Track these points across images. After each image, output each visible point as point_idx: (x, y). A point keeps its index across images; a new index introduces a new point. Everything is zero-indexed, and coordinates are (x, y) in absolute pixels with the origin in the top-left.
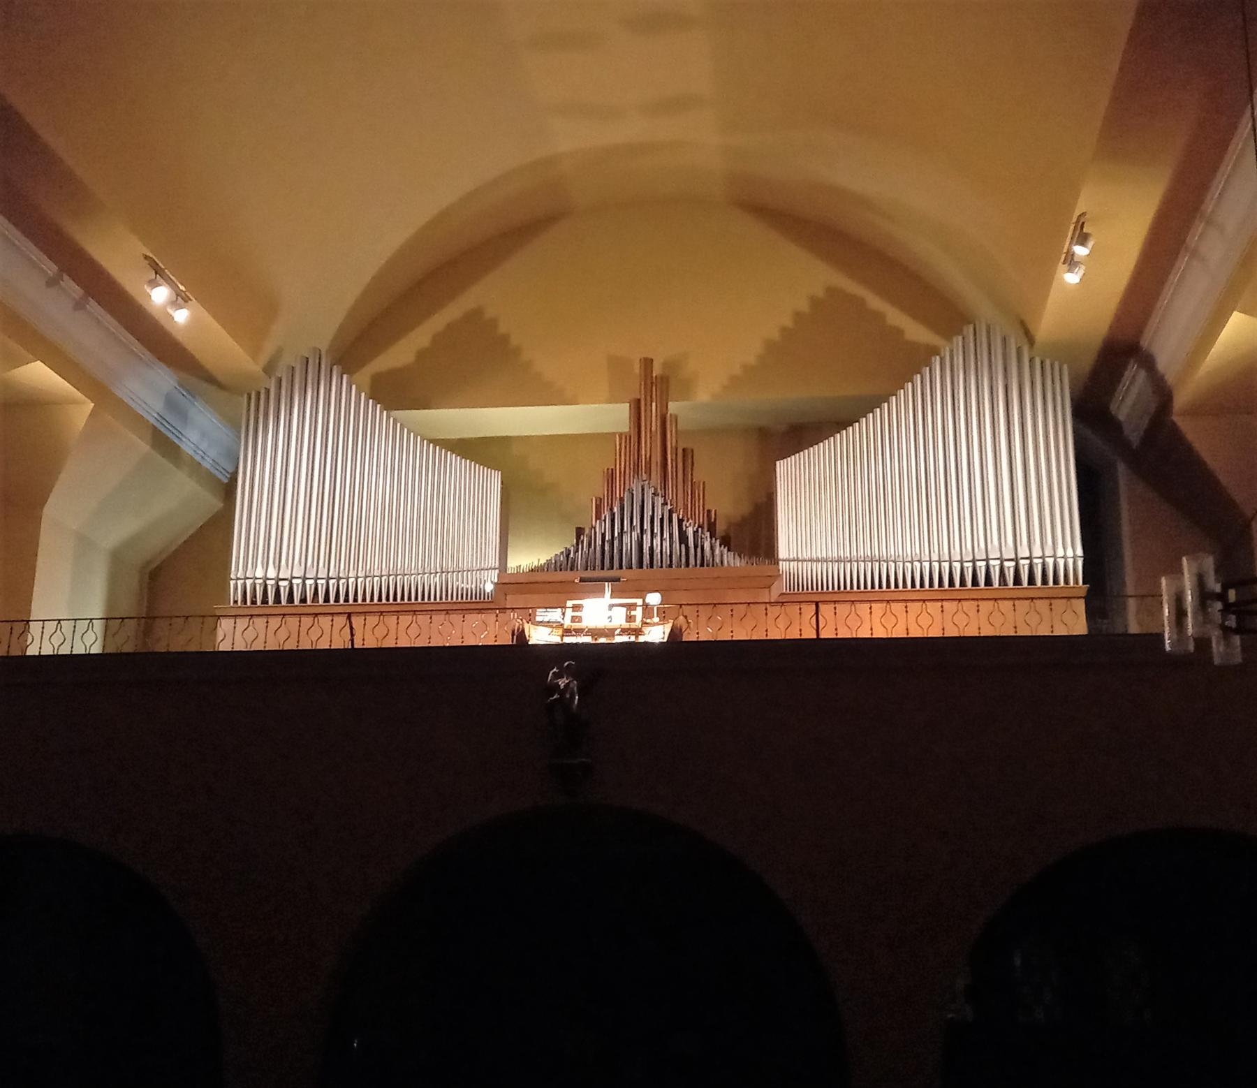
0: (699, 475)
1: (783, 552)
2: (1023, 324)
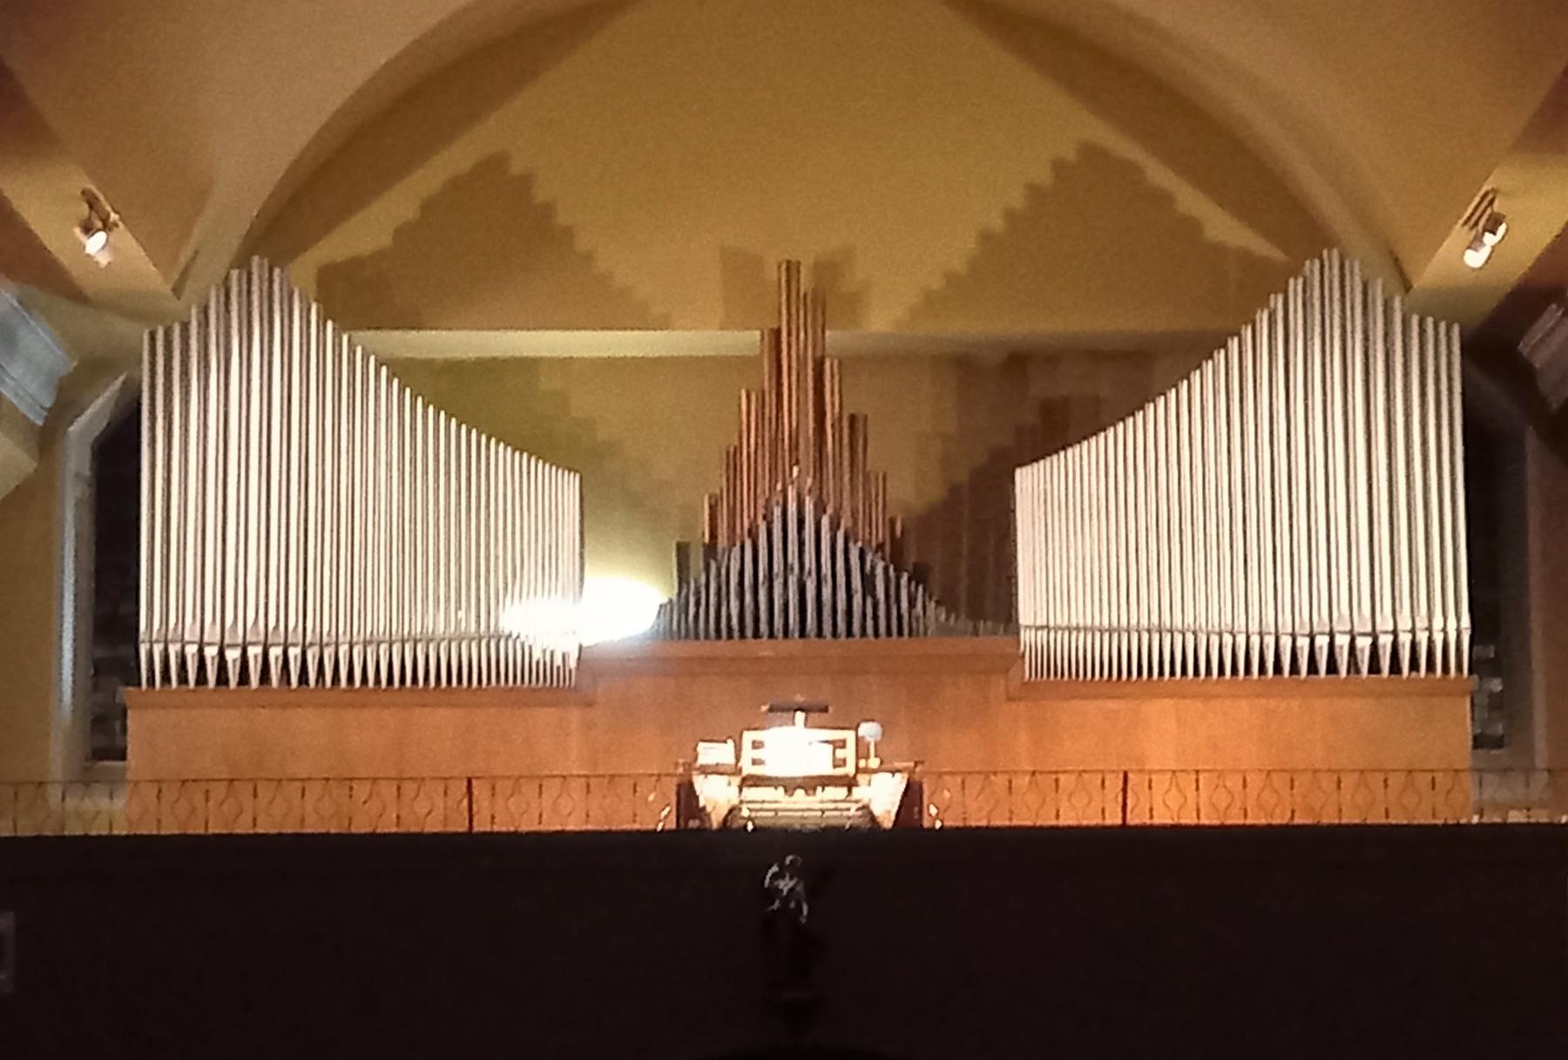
0: (875, 459)
1: (1025, 615)
2: (1397, 262)
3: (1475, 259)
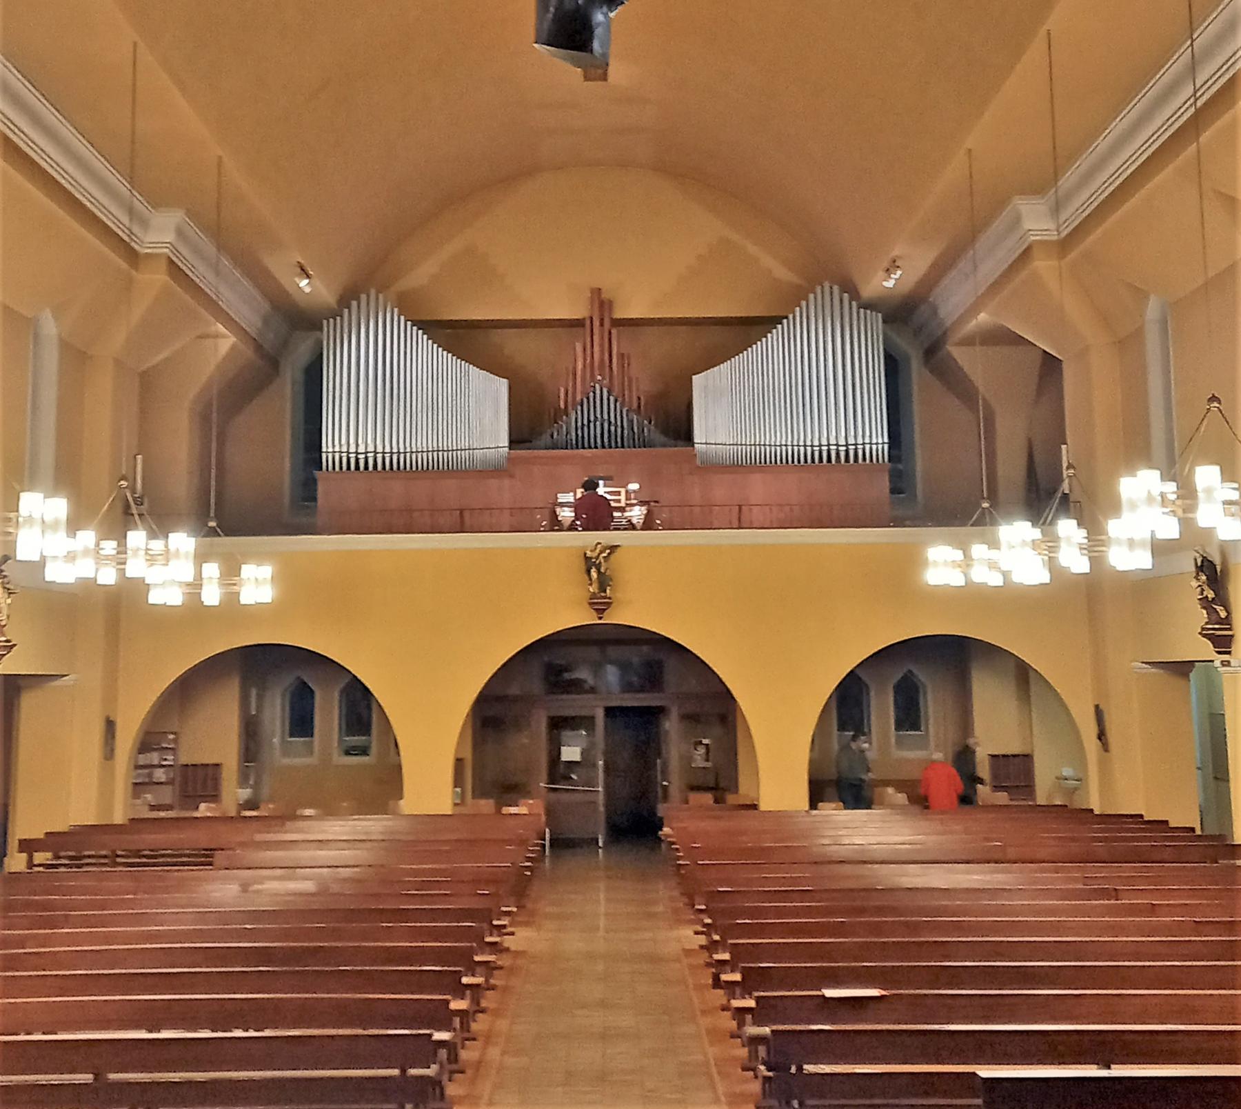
1: (698, 437)
3: (890, 284)
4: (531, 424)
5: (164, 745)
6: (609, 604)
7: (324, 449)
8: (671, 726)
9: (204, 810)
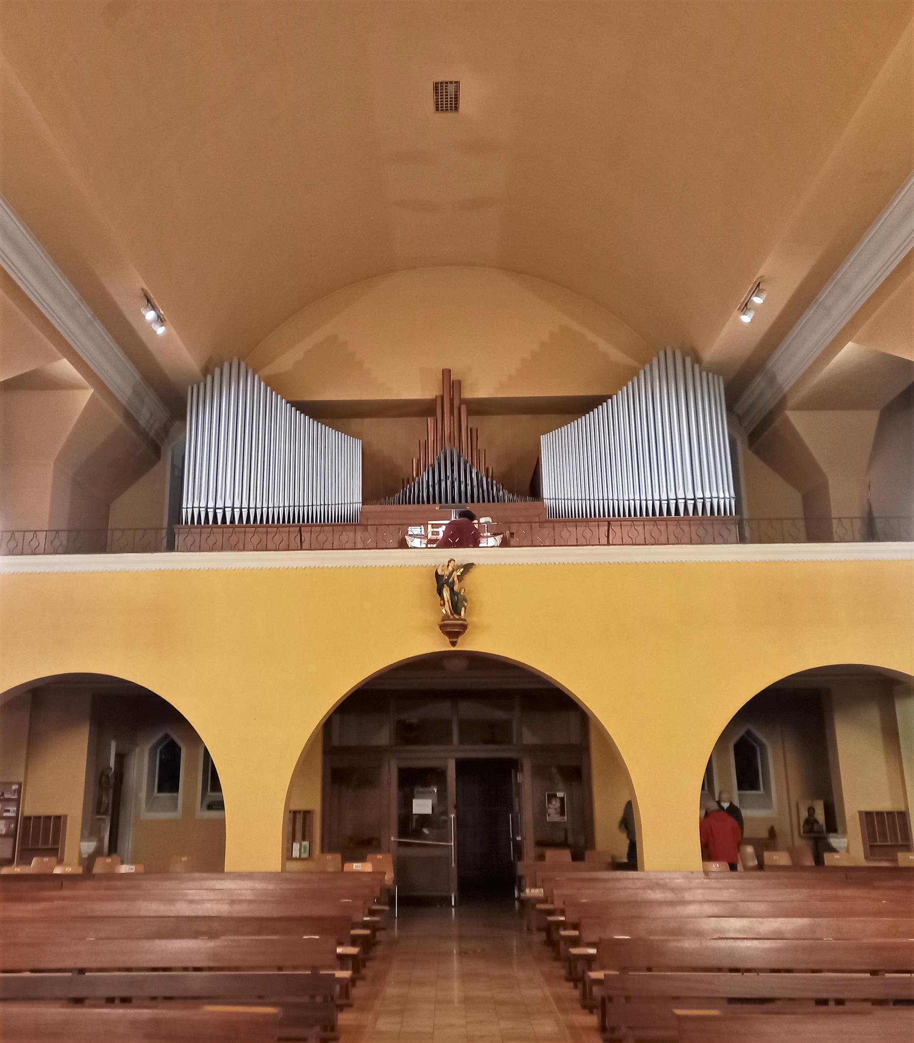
1: (547, 491)
4: (383, 482)
5: (7, 796)
6: (464, 627)
7: (184, 506)
8: (525, 779)
9: (35, 865)
